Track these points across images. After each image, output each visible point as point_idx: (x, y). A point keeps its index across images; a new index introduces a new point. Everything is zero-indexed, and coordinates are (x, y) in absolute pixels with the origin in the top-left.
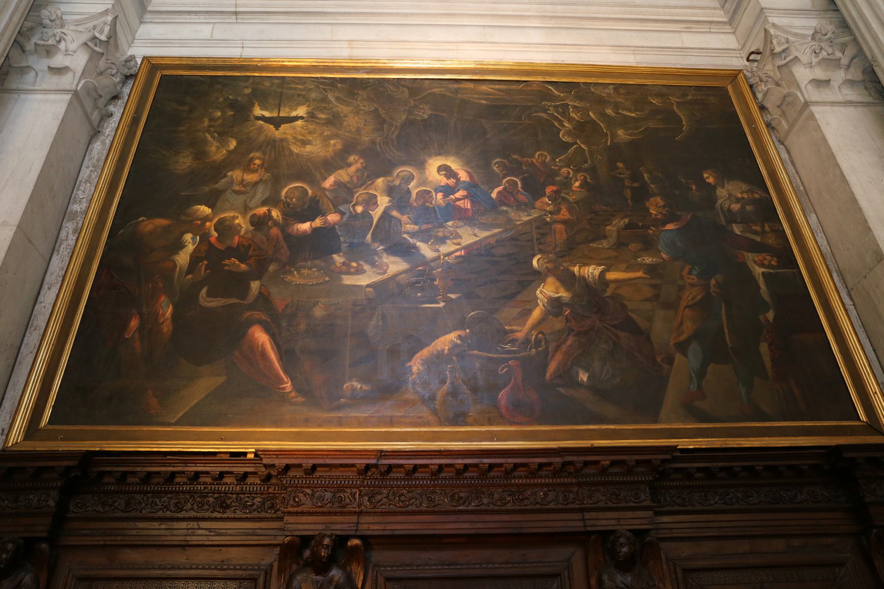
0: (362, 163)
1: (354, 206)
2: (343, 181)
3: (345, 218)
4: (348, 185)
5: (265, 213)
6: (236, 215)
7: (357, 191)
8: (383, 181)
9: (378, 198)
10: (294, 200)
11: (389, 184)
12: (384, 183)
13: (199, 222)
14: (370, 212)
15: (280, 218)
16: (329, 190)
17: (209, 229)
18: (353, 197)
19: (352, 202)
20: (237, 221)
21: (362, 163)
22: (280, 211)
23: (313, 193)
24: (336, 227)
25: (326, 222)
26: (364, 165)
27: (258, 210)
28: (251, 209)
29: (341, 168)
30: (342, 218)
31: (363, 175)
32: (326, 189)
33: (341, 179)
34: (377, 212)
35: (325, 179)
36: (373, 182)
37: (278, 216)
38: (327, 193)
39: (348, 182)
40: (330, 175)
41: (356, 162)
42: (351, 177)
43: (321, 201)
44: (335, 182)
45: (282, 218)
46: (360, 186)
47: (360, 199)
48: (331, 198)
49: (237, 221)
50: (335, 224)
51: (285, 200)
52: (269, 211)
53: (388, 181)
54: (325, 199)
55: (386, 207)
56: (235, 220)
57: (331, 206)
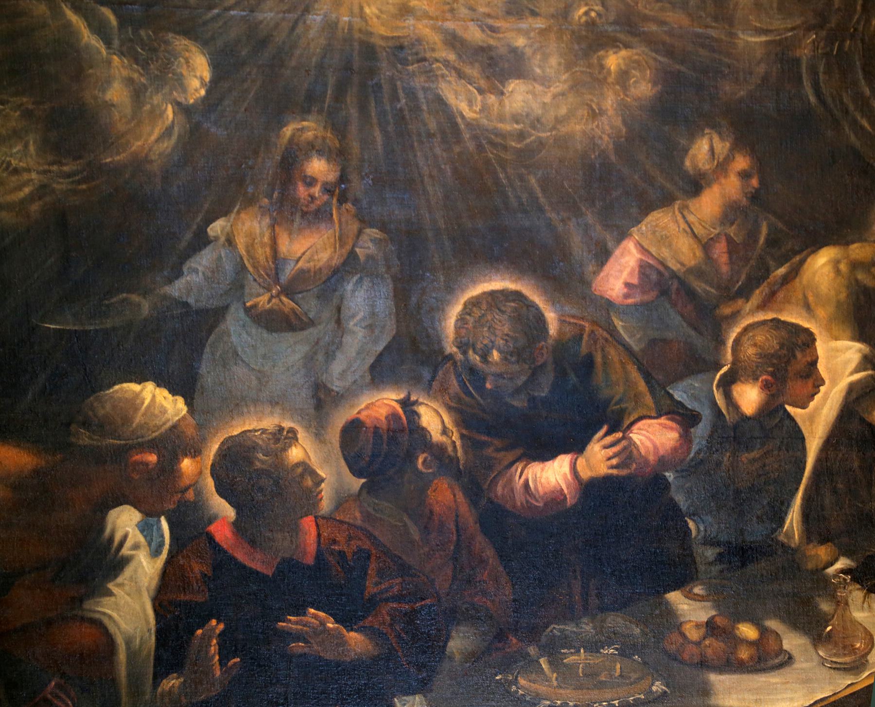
0: (744, 175)
1: (728, 382)
2: (673, 265)
3: (701, 430)
4: (699, 286)
5: (393, 417)
6: (287, 424)
7: (735, 316)
8: (836, 263)
9: (821, 347)
10: (496, 355)
11: (861, 276)
12: (838, 271)
13: (153, 458)
14: (789, 408)
15: (455, 437)
16: (624, 311)
17: (195, 485)
18: (720, 342)
19: (719, 367)
20: (295, 454)
21: (744, 175)
22: (449, 408)
23: (562, 321)
24: (670, 476)
25: (628, 454)
26: (755, 182)
27: (364, 401)
28: (338, 399)
29: (666, 201)
30: (686, 438)
31: (753, 235)
32: (609, 305)
33: (665, 253)
34: (817, 409)
35: (603, 255)
36: (795, 272)
37: (445, 431)
38: (619, 324)
39: (698, 272)
40: (622, 235)
41: (722, 168)
42: (706, 246)
43: (599, 359)
44: (643, 268)
45: (462, 436)
46: (745, 293)
47: (750, 351)
48: (636, 348)
49: (295, 454)
50: (663, 462)
51: (460, 356)
52: (406, 403)
53: (855, 265)
54: (613, 353)
55: (851, 387)
56: (285, 449)
57: (642, 386)
